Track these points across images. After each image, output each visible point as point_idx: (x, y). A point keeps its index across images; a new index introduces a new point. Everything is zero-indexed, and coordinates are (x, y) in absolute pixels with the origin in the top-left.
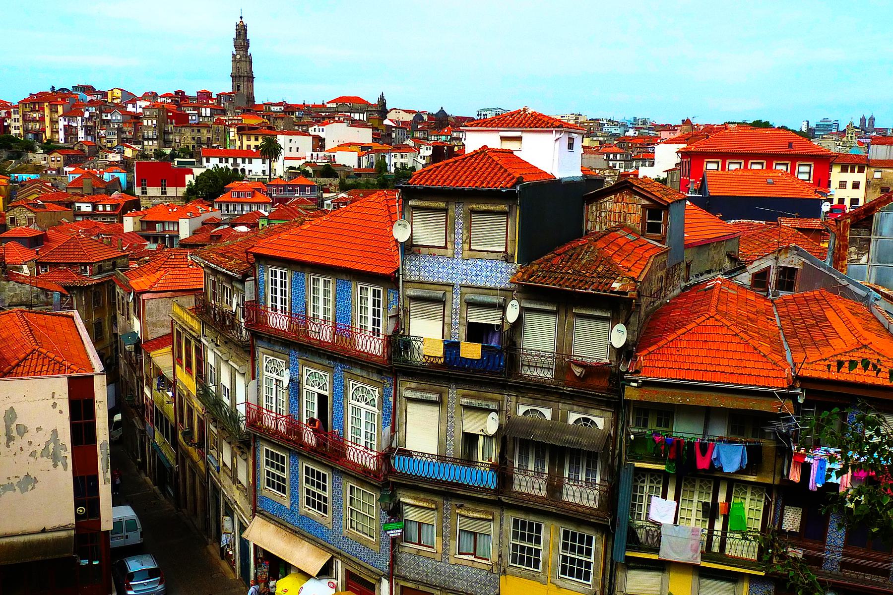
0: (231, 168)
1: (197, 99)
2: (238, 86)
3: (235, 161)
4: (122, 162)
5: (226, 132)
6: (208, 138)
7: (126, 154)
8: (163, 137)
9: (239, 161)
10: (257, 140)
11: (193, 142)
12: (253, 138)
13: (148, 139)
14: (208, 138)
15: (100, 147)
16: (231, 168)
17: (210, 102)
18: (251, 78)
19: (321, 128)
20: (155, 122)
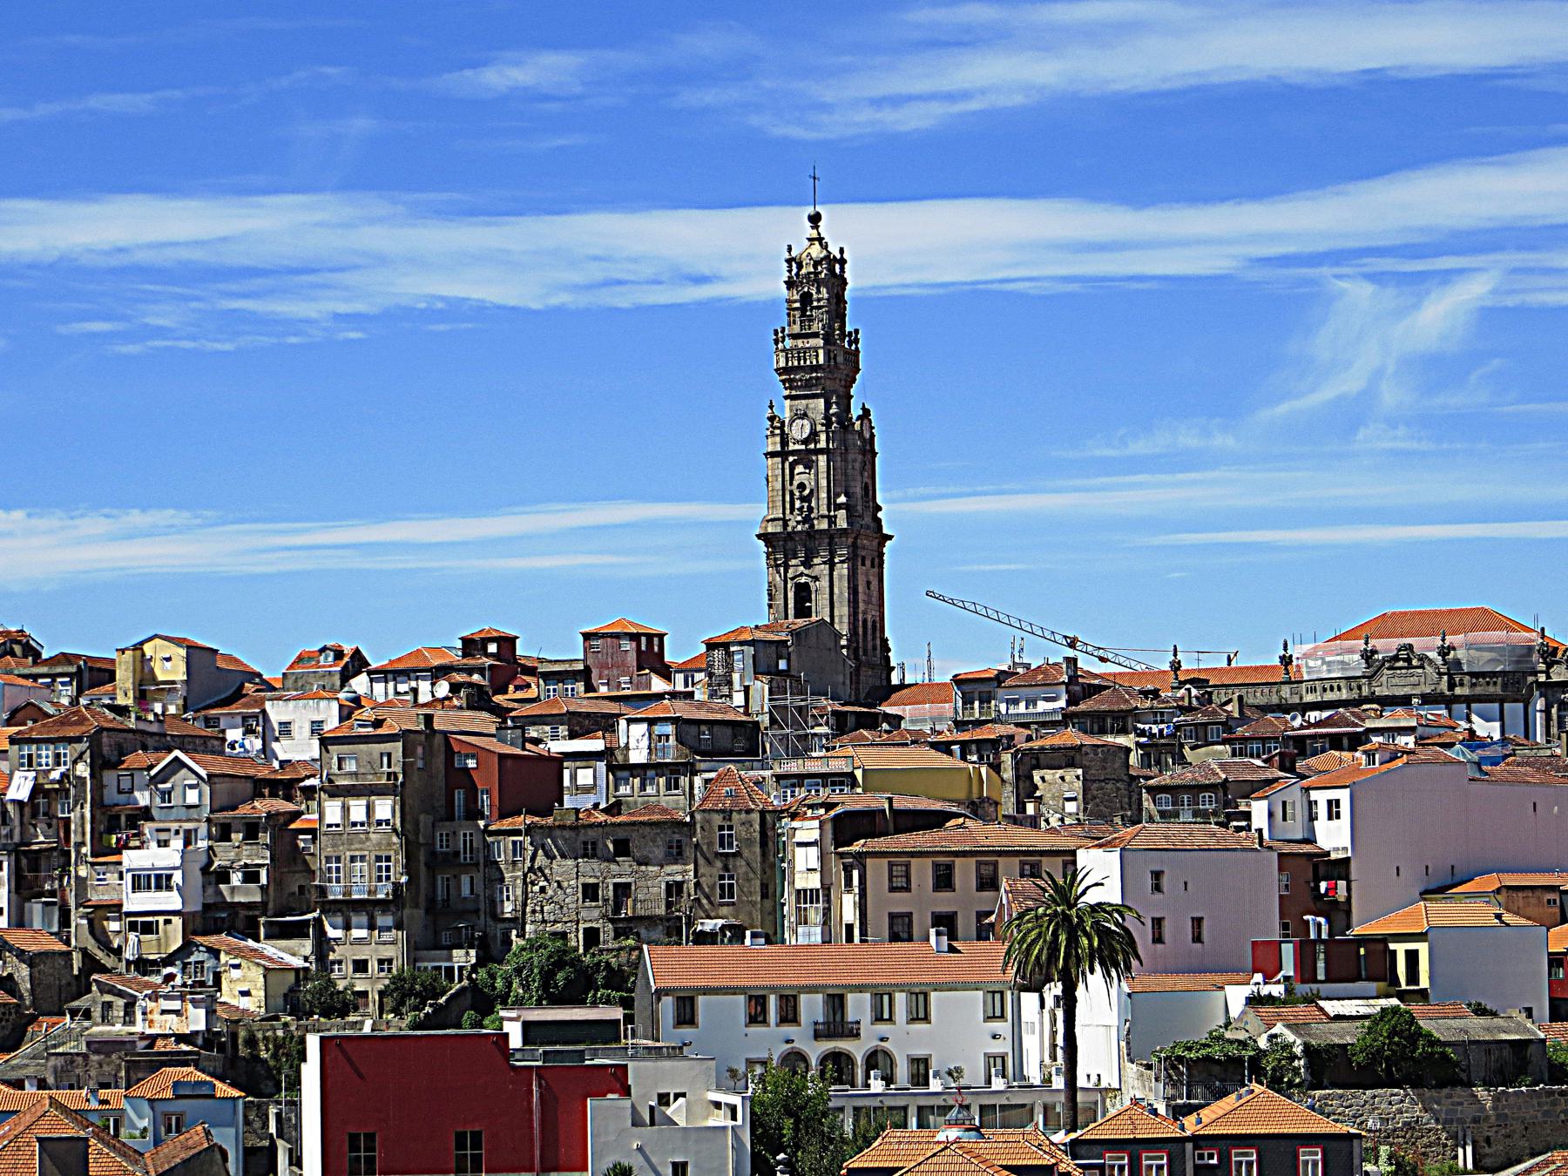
0: (815, 1051)
1: (585, 675)
2: (803, 592)
3: (836, 1002)
4: (209, 1039)
5: (771, 845)
6: (675, 889)
7: (228, 995)
8: (442, 893)
9: (858, 1007)
10: (944, 880)
11: (592, 916)
12: (922, 873)
13: (347, 909)
14: (675, 889)
15: (92, 965)
16: (815, 1051)
17: (658, 685)
18: (864, 542)
19: (1321, 797)
20: (384, 808)
